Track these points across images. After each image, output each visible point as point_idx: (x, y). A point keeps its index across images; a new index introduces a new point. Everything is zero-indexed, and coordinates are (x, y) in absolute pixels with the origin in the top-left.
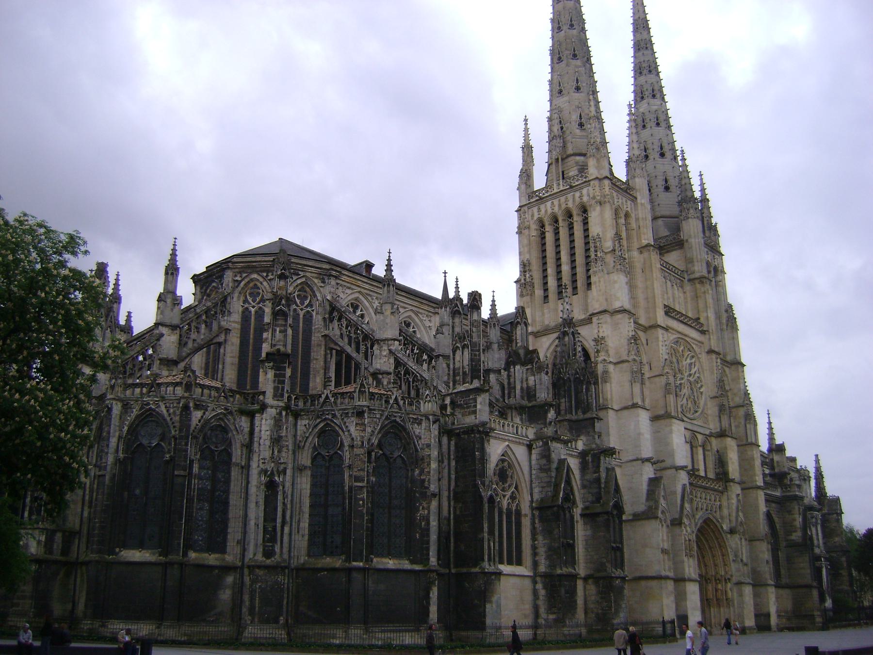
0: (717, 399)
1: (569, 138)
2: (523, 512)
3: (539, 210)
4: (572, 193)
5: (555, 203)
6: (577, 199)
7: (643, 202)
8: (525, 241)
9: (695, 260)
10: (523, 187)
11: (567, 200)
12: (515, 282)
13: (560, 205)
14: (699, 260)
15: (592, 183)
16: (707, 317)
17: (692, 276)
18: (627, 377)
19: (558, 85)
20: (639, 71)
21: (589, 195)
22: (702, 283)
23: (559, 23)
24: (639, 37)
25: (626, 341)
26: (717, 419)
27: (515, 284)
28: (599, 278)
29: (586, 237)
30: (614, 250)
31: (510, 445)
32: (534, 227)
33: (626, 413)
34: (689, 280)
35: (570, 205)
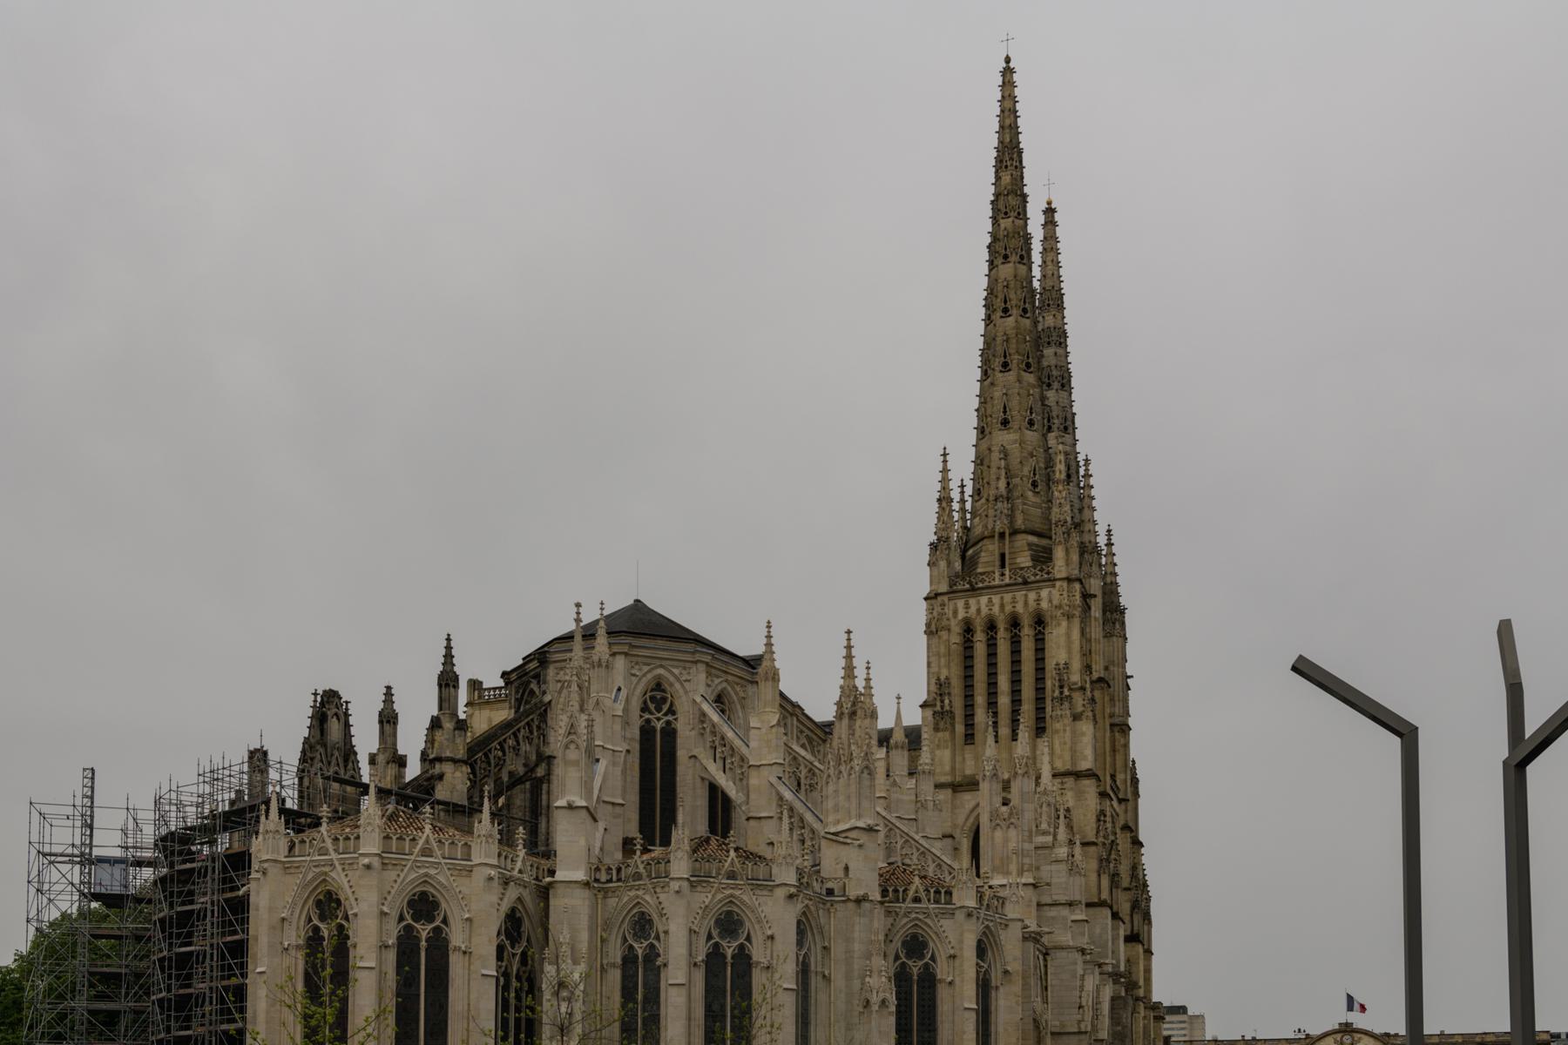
0: (1129, 892)
3: (967, 606)
4: (1024, 592)
5: (994, 601)
6: (1032, 603)
7: (1097, 615)
8: (943, 650)
9: (1116, 698)
11: (1014, 601)
12: (921, 706)
13: (1002, 606)
14: (1121, 698)
15: (1058, 584)
21: (1050, 601)
25: (1094, 817)
27: (920, 709)
28: (1065, 725)
30: (1083, 689)
32: (956, 629)
35: (1020, 608)
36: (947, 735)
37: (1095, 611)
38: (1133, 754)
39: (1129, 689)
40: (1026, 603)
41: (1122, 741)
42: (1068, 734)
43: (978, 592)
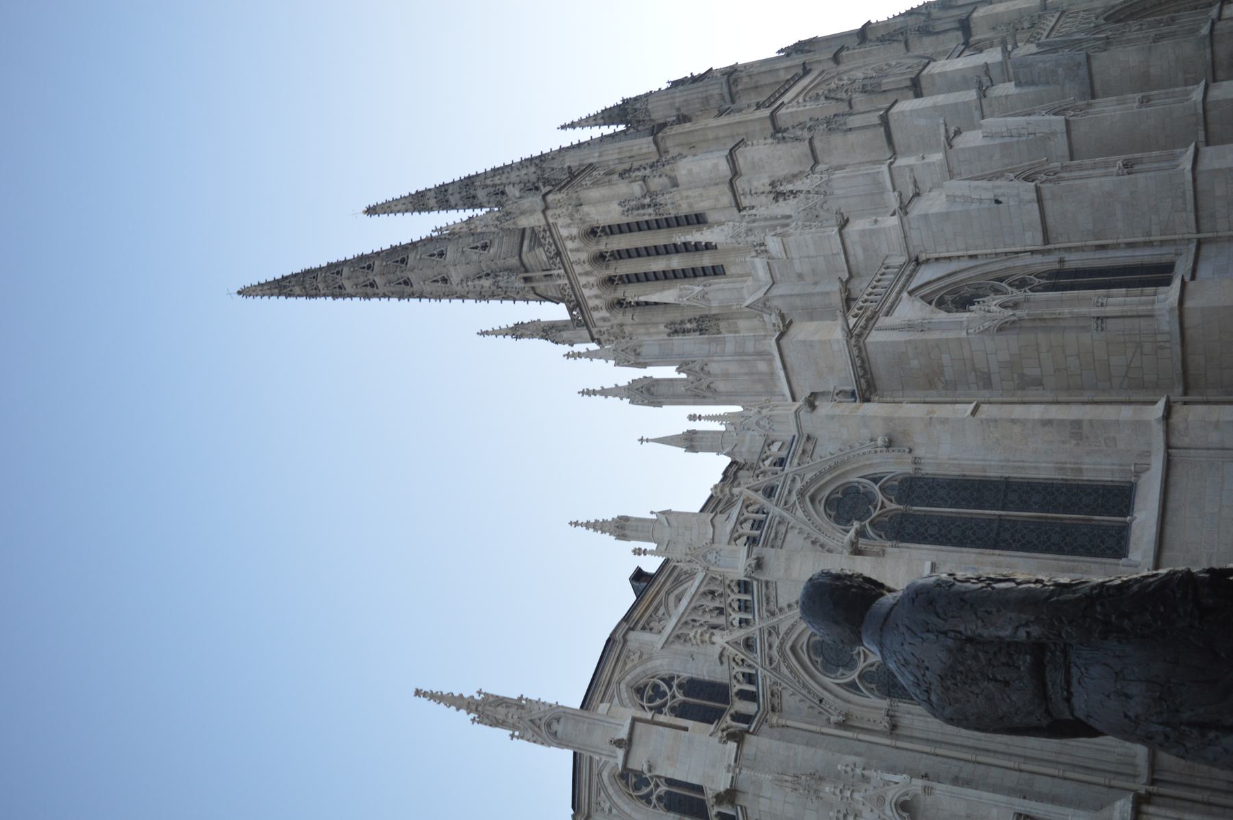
0: (910, 41)
1: (500, 263)
2: (1056, 266)
3: (596, 308)
4: (569, 253)
5: (584, 282)
7: (597, 154)
10: (565, 334)
11: (578, 263)
13: (587, 274)
14: (705, 89)
15: (551, 221)
16: (787, 68)
17: (727, 97)
18: (837, 139)
19: (436, 284)
20: (471, 200)
21: (569, 226)
22: (736, 80)
23: (366, 286)
24: (432, 202)
25: (779, 146)
26: (941, 37)
28: (682, 198)
29: (629, 228)
30: (644, 179)
31: (911, 288)
33: (897, 136)
34: (733, 101)
35: (584, 256)
36: (722, 324)
37: (594, 157)
38: (773, 54)
39: (711, 69)
40: (578, 250)
41: (746, 80)
42: (690, 193)
43: (580, 300)
